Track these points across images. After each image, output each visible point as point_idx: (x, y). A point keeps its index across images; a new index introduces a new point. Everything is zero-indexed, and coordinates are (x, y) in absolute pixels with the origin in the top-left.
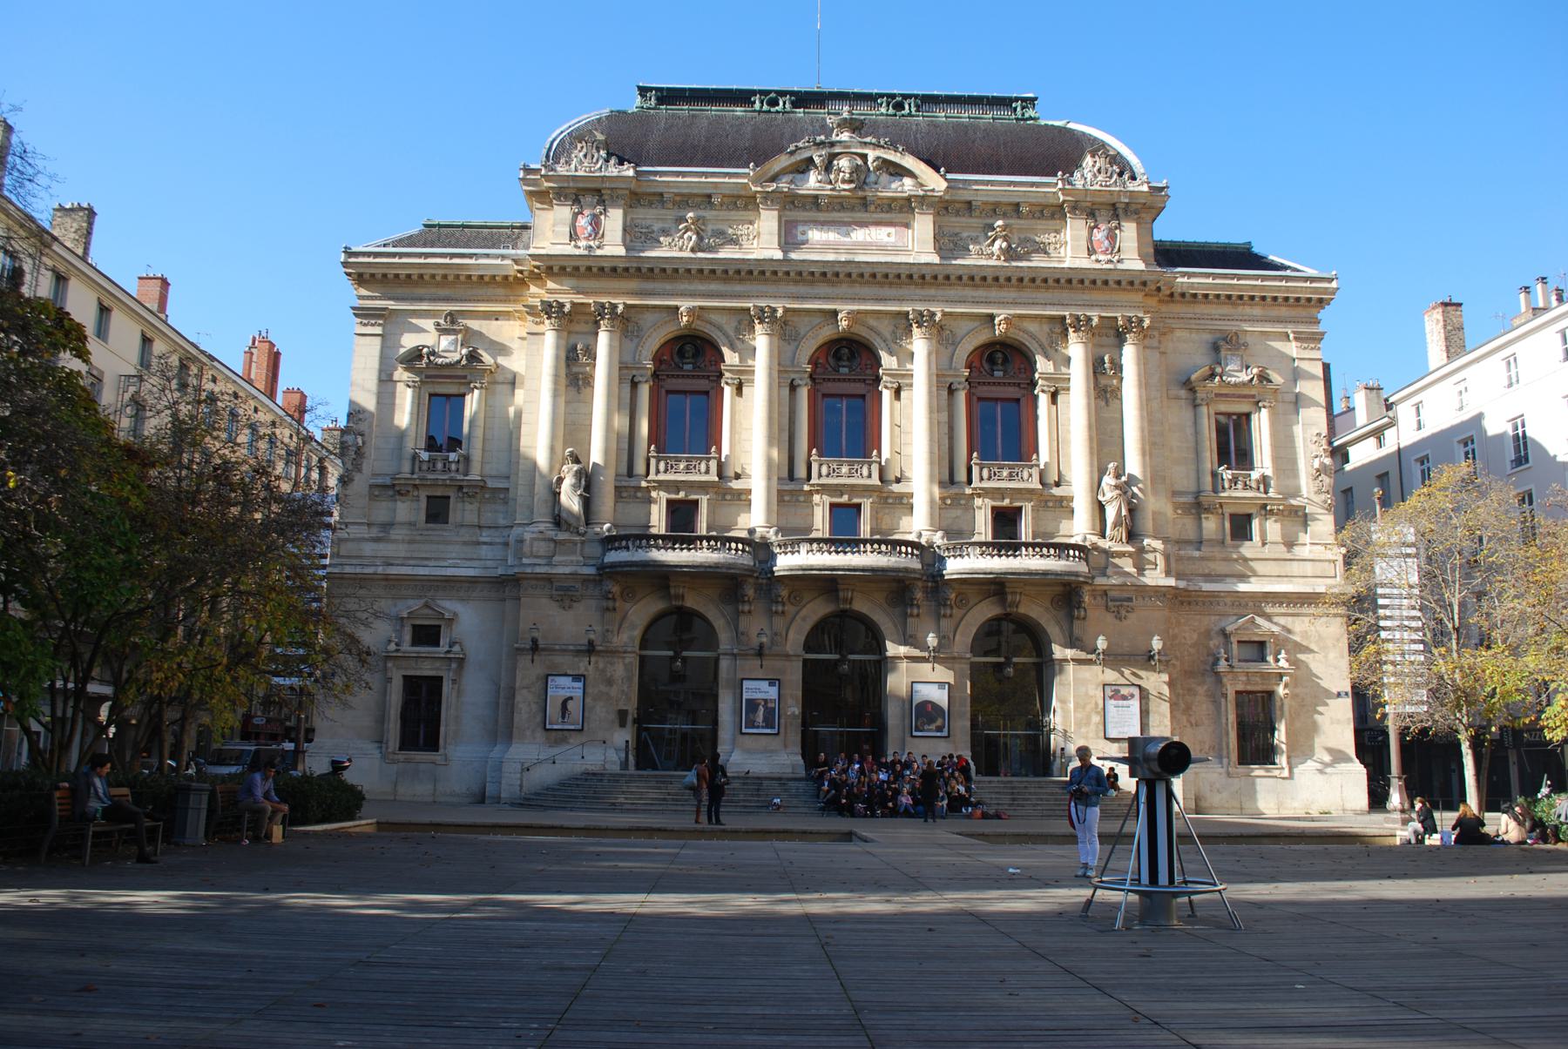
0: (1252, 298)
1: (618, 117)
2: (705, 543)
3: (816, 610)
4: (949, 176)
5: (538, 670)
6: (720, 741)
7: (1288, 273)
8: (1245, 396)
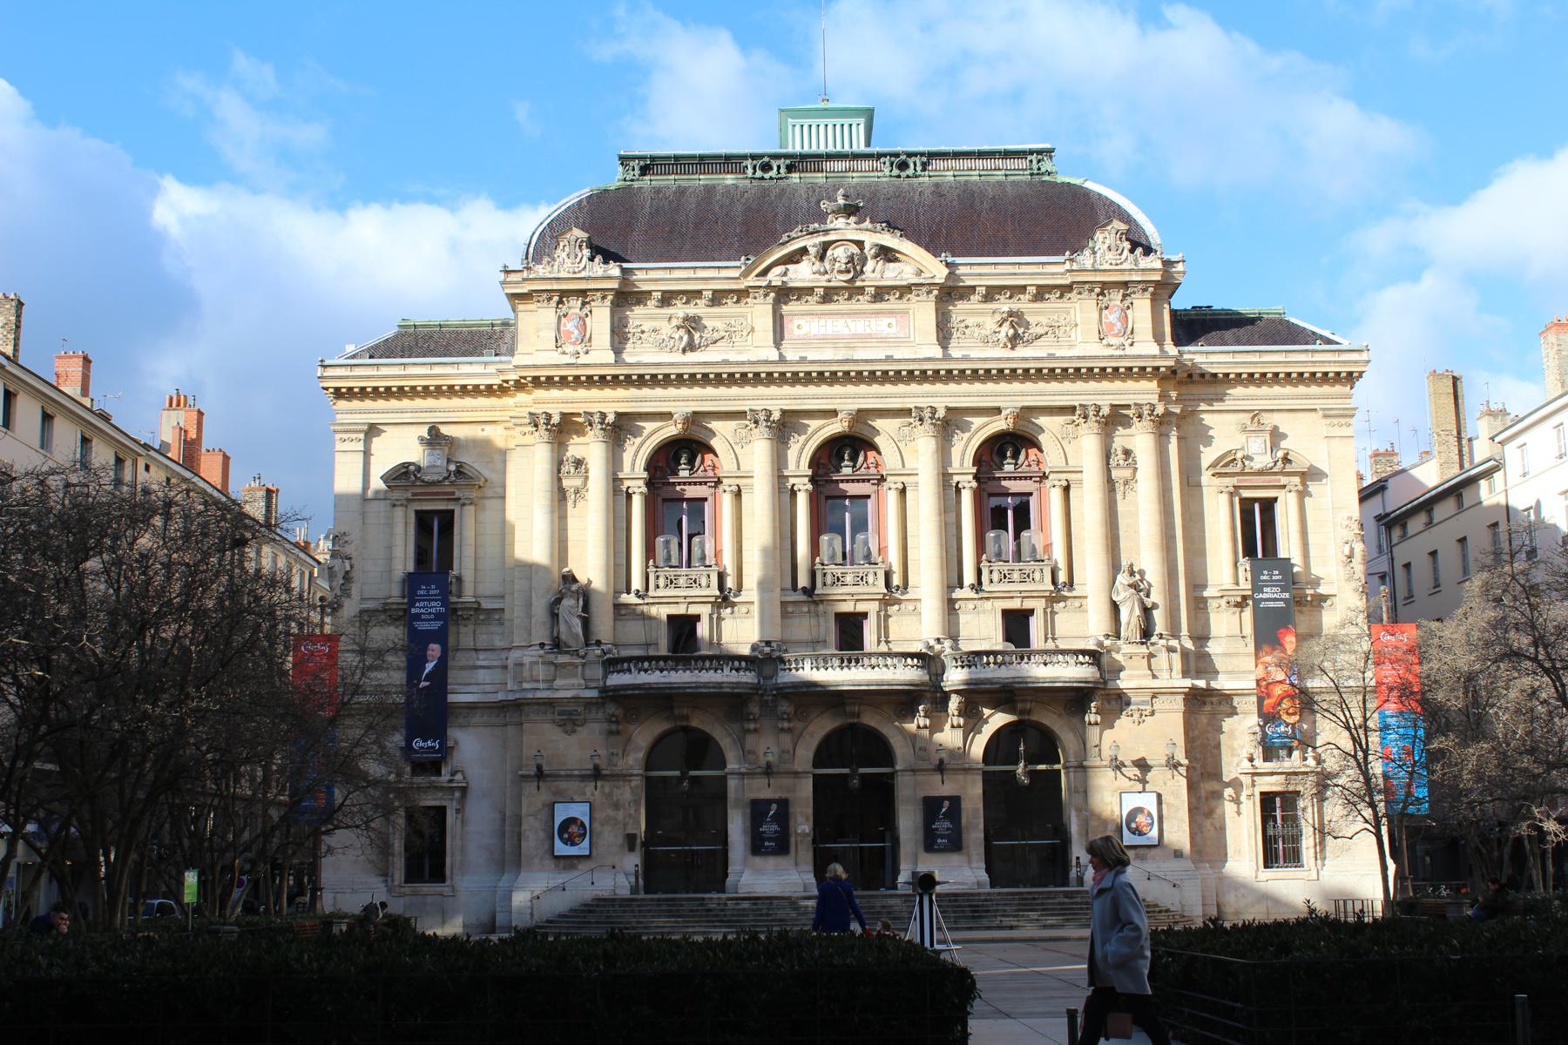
1: (599, 200)
2: (707, 664)
3: (822, 726)
5: (544, 796)
6: (730, 862)
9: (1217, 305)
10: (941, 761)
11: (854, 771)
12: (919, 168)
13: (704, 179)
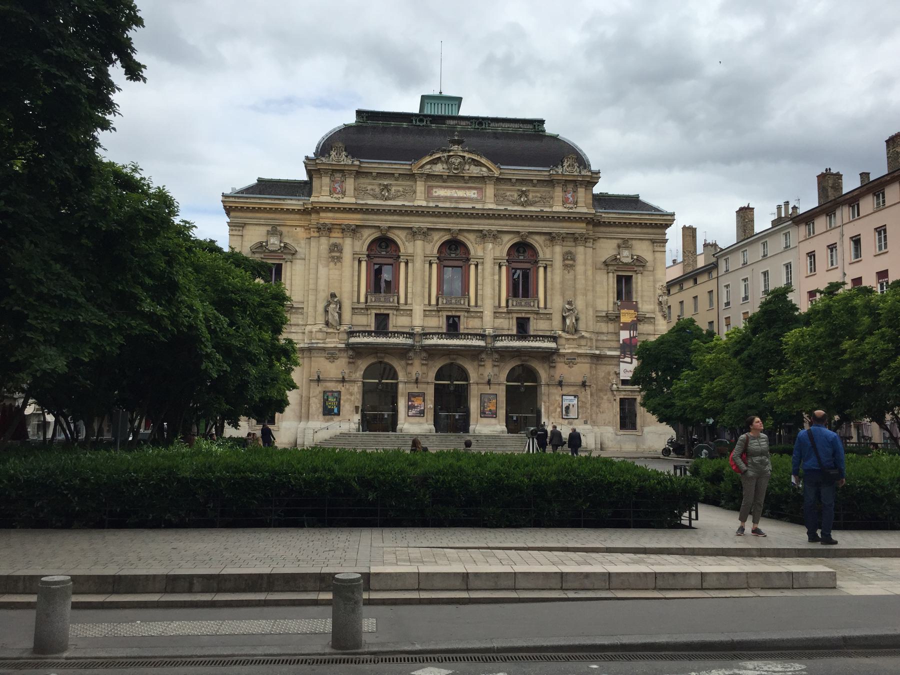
9: (610, 193)
10: (489, 380)
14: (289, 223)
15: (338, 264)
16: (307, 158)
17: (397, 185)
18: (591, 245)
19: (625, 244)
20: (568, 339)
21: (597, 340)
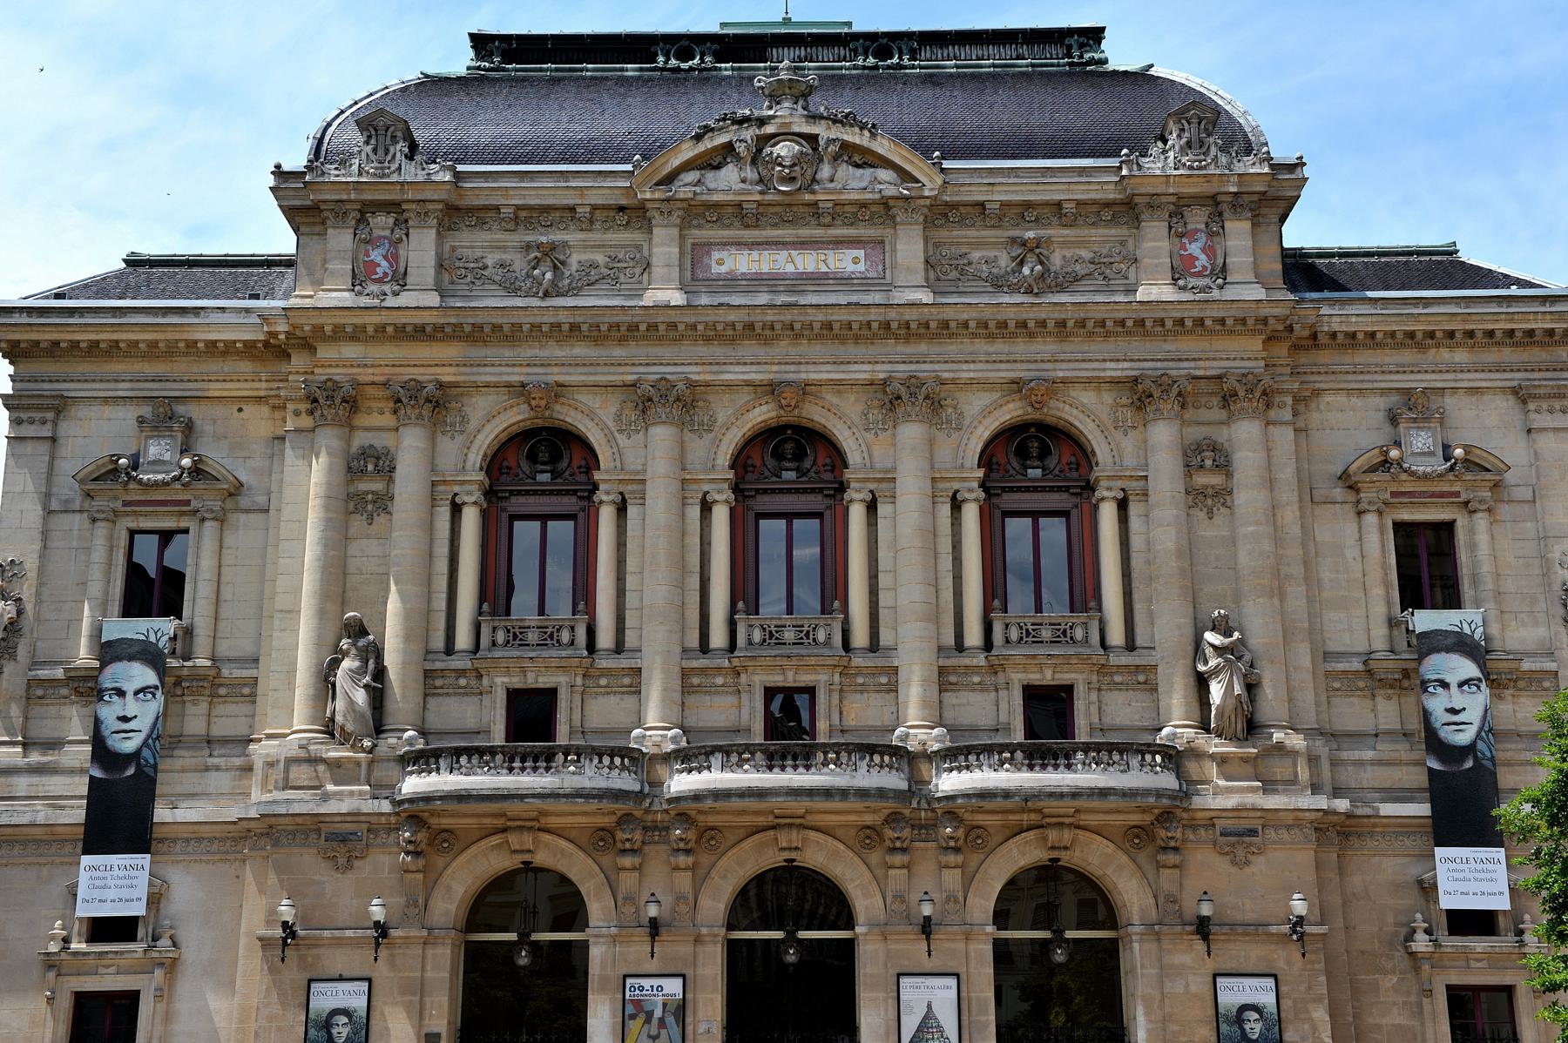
0: (1451, 334)
4: (946, 164)
7: (1514, 290)
8: (1442, 495)
11: (791, 934)
12: (906, 57)
13: (590, 69)
14: (215, 389)
15: (381, 520)
16: (278, 172)
17: (586, 247)
18: (1287, 415)
19: (1411, 407)
20: (1222, 760)
21: (1334, 763)
